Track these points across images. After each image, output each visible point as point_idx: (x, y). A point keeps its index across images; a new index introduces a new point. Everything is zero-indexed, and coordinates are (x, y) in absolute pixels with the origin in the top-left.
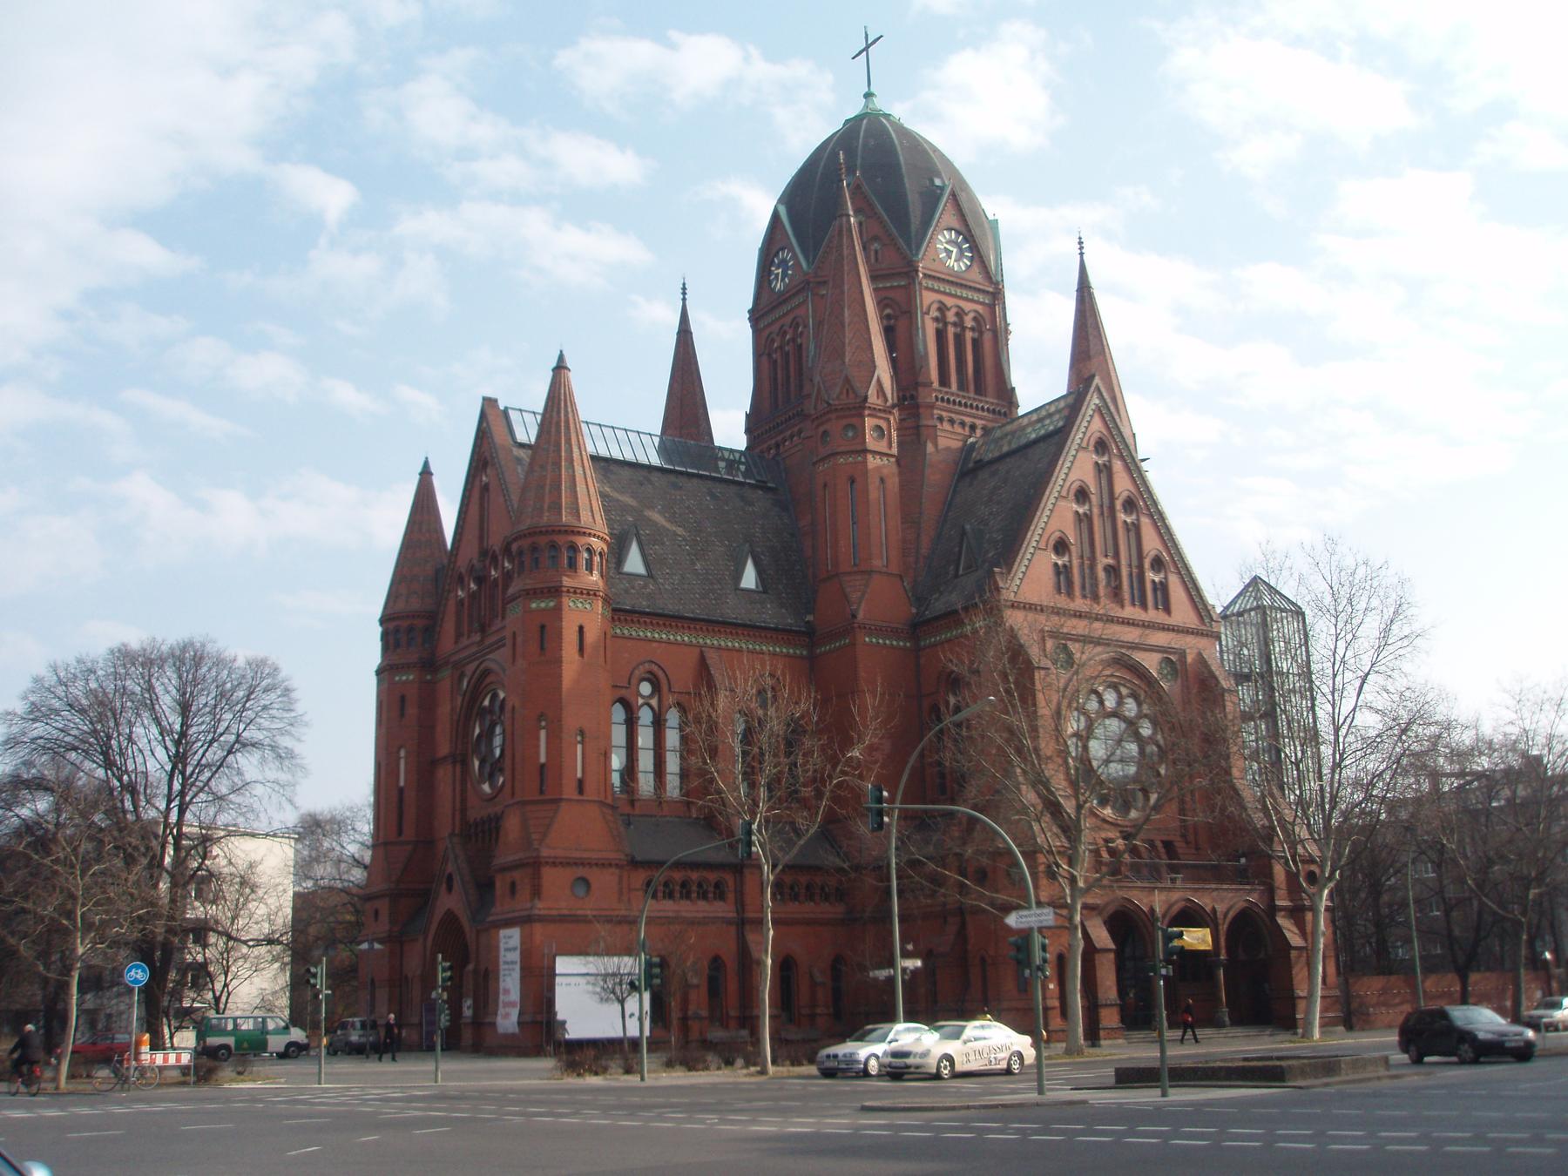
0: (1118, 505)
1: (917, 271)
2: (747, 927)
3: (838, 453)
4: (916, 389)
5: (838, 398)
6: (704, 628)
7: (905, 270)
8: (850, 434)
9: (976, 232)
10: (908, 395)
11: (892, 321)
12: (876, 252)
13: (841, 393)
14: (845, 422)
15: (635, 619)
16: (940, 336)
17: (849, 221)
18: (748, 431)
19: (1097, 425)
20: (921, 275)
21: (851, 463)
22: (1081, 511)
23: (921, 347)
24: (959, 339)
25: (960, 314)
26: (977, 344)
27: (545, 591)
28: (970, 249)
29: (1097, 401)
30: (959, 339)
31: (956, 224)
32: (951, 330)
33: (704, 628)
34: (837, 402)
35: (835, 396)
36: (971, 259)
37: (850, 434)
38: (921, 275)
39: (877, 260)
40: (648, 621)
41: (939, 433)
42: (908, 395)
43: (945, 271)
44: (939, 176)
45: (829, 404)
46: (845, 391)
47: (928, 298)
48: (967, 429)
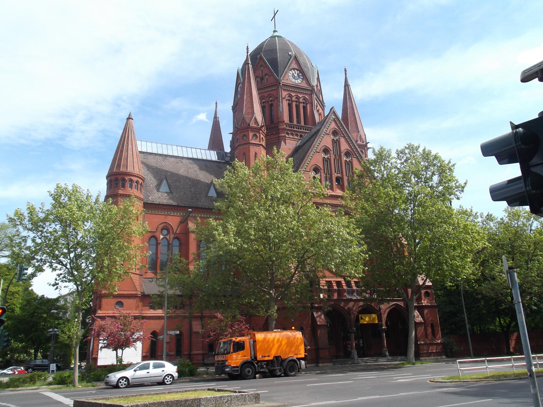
0: (342, 154)
1: (280, 83)
4: (278, 123)
5: (240, 125)
7: (276, 83)
8: (245, 138)
9: (305, 70)
10: (276, 126)
11: (272, 102)
12: (267, 79)
13: (241, 124)
14: (242, 134)
15: (160, 207)
16: (290, 105)
17: (248, 66)
18: (231, 146)
19: (333, 126)
20: (281, 85)
21: (244, 148)
22: (326, 157)
23: (281, 109)
24: (297, 107)
25: (298, 98)
26: (305, 108)
27: (113, 195)
28: (302, 75)
29: (334, 117)
30: (297, 107)
31: (296, 67)
32: (294, 104)
34: (240, 127)
36: (303, 79)
37: (245, 138)
38: (281, 85)
39: (267, 81)
40: (165, 207)
41: (287, 138)
44: (291, 51)
45: (237, 128)
47: (285, 94)
48: (299, 137)
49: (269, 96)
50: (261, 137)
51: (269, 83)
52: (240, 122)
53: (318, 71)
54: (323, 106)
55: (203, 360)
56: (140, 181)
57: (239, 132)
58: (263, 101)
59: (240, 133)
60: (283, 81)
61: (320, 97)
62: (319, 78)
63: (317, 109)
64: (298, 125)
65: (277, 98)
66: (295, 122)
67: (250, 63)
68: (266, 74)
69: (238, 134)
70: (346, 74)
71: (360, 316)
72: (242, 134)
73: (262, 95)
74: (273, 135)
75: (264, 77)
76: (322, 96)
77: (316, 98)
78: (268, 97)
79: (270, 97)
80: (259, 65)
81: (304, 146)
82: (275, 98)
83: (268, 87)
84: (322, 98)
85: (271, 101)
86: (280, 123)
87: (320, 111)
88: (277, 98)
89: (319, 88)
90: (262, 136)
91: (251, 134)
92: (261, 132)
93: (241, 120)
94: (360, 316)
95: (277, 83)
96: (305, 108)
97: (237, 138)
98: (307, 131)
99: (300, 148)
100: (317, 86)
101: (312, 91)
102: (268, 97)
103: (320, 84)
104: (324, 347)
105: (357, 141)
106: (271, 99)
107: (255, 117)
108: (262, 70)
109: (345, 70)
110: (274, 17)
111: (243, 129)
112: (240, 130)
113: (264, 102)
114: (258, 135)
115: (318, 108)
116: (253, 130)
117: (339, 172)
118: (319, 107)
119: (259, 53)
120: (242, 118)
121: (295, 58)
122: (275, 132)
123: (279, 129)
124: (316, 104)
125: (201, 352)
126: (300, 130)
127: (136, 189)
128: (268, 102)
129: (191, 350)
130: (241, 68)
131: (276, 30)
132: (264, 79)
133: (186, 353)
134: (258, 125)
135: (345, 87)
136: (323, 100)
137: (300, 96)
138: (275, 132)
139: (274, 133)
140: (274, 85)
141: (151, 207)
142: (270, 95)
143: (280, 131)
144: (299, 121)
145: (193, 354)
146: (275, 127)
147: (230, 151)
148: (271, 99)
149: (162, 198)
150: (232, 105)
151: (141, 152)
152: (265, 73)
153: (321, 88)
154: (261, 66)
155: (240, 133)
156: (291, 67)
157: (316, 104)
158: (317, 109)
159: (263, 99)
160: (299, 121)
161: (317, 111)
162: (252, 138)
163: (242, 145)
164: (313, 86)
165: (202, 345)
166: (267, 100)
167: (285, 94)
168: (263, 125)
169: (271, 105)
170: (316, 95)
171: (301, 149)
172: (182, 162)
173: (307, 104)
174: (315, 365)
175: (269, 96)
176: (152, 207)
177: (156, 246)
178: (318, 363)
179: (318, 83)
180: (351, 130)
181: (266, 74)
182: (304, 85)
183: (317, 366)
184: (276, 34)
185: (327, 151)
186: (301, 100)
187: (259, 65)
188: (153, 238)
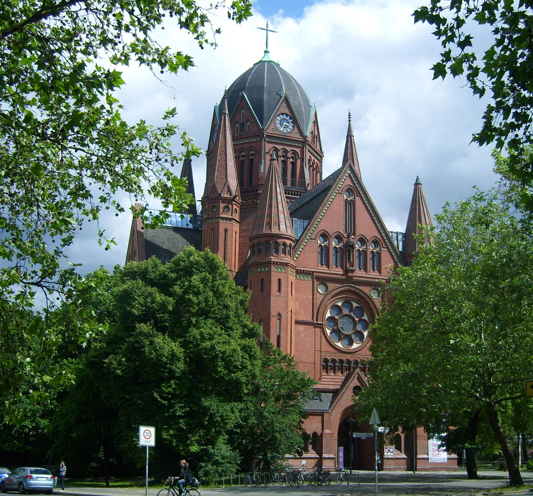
8: (215, 210)
20: (265, 136)
26: (294, 164)
31: (287, 112)
37: (215, 210)
38: (265, 136)
47: (268, 147)
50: (234, 209)
53: (316, 112)
54: (321, 157)
58: (243, 153)
60: (269, 131)
70: (350, 121)
85: (252, 155)
88: (259, 152)
90: (235, 207)
91: (222, 205)
92: (234, 203)
95: (260, 134)
96: (294, 164)
101: (304, 142)
109: (349, 115)
114: (230, 206)
121: (286, 100)
124: (308, 157)
134: (231, 195)
137: (288, 149)
148: (252, 152)
150: (207, 150)
162: (223, 211)
164: (306, 137)
167: (268, 147)
169: (252, 160)
173: (296, 160)
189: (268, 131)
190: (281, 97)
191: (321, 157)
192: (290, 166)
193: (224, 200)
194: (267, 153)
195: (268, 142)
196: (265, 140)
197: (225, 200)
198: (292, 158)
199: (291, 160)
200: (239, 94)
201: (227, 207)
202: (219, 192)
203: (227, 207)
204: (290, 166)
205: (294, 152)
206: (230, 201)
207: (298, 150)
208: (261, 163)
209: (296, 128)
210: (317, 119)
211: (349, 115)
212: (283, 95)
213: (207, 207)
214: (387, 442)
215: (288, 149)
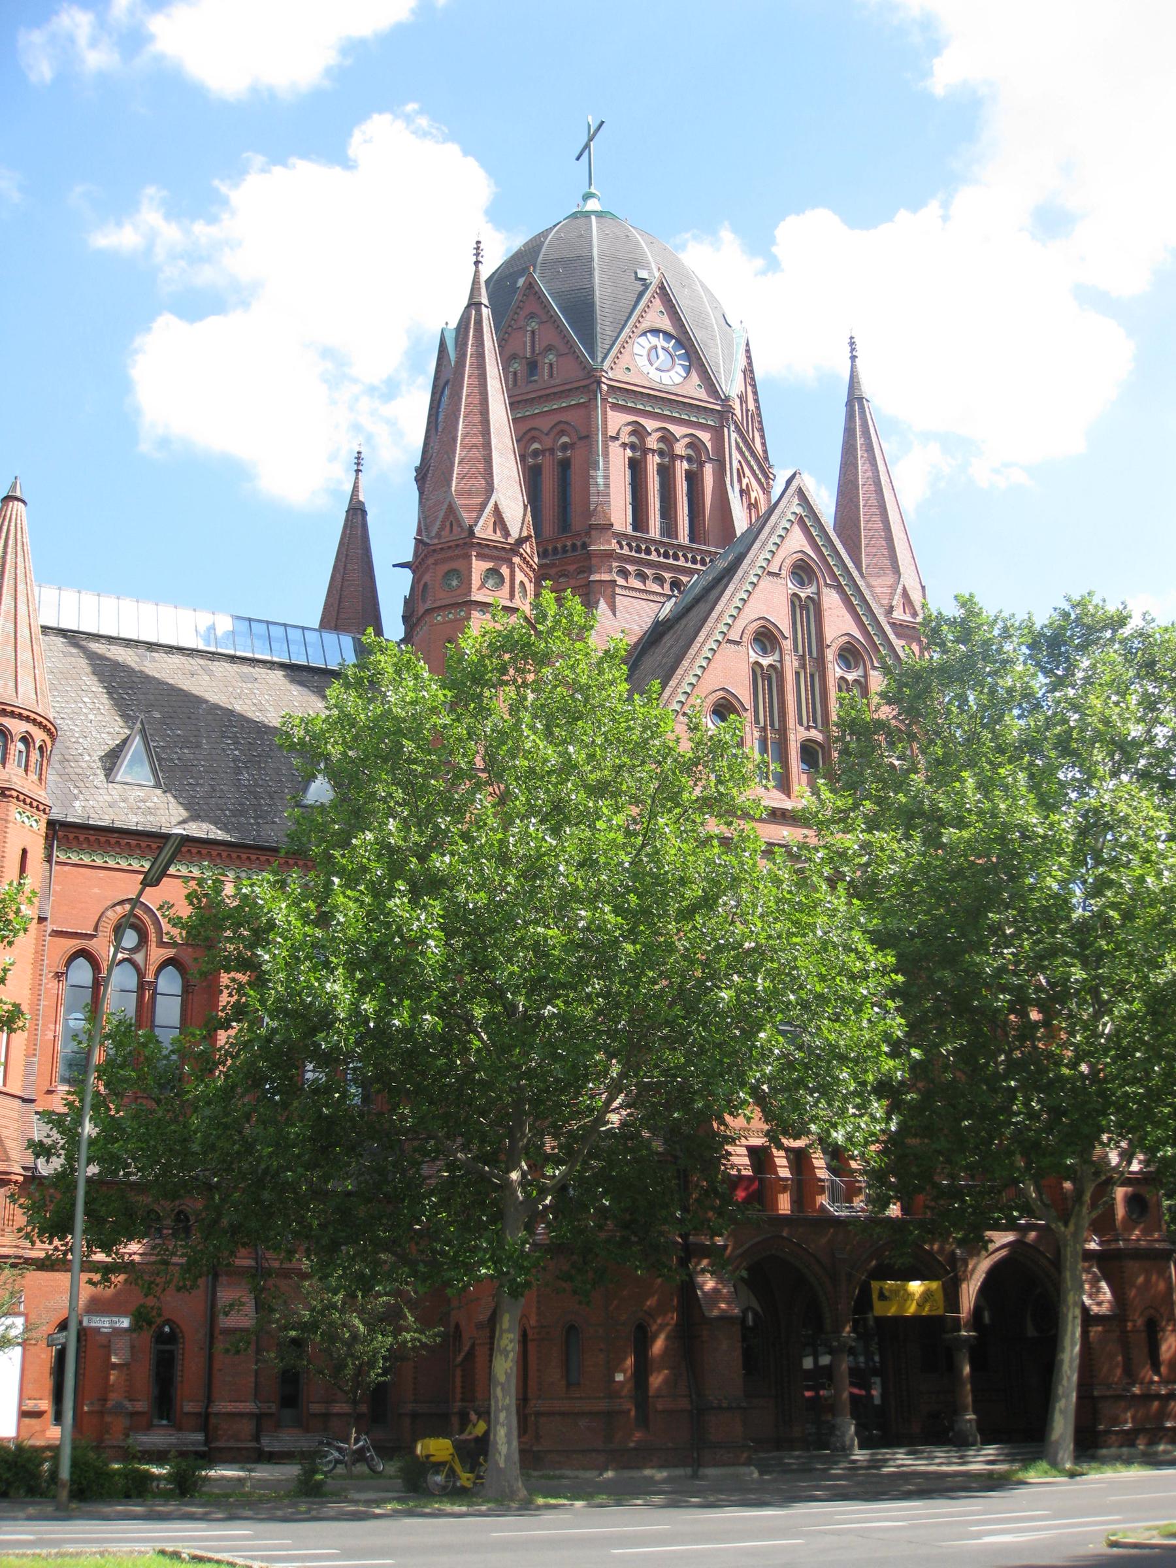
0: (830, 654)
1: (599, 382)
2: (223, 1279)
3: (433, 610)
4: (588, 534)
5: (438, 535)
6: (224, 854)
8: (455, 583)
9: (698, 335)
10: (579, 543)
11: (569, 453)
12: (551, 365)
13: (442, 528)
14: (446, 567)
15: (113, 841)
16: (636, 467)
17: (479, 314)
18: (406, 619)
19: (797, 541)
20: (605, 387)
21: (452, 621)
22: (765, 662)
23: (600, 480)
24: (666, 473)
25: (667, 438)
26: (694, 479)
28: (688, 356)
29: (799, 510)
30: (666, 473)
31: (666, 324)
32: (653, 461)
33: (224, 854)
34: (436, 541)
35: (433, 534)
36: (688, 371)
37: (455, 583)
38: (605, 387)
39: (551, 375)
40: (133, 842)
41: (618, 591)
42: (579, 543)
43: (646, 384)
44: (646, 266)
46: (448, 524)
47: (617, 421)
48: (667, 586)
49: (558, 428)
50: (517, 582)
51: (557, 381)
52: (438, 523)
53: (748, 345)
54: (767, 477)
55: (257, 1439)
56: (39, 736)
57: (430, 561)
58: (536, 446)
59: (436, 563)
60: (613, 372)
61: (753, 440)
62: (752, 371)
63: (740, 481)
64: (665, 540)
65: (587, 437)
66: (655, 530)
67: (485, 300)
68: (549, 348)
69: (428, 568)
70: (853, 358)
71: (875, 1285)
72: (446, 567)
73: (529, 424)
74: (566, 576)
75: (539, 358)
76: (763, 437)
77: (737, 444)
78: (555, 431)
79: (562, 433)
80: (523, 314)
81: (683, 622)
82: (581, 439)
83: (555, 394)
84: (764, 444)
85: (565, 447)
86: (593, 533)
87: (753, 495)
88: (586, 438)
89: (751, 406)
90: (519, 576)
91: (479, 567)
92: (516, 560)
93: (441, 514)
94: (875, 1285)
95: (590, 381)
96: (694, 479)
97: (426, 584)
98: (698, 566)
99: (670, 628)
100: (743, 399)
101: (724, 414)
102: (555, 431)
103: (755, 393)
104: (725, 1405)
105: (890, 610)
106: (565, 439)
107: (496, 506)
108: (533, 332)
109: (852, 344)
110: (587, 146)
111: (450, 547)
112: (434, 551)
113: (536, 453)
114: (505, 571)
115: (745, 481)
116: (486, 551)
117: (815, 721)
118: (748, 479)
119: (524, 271)
120: (445, 506)
121: (664, 293)
122: (575, 567)
123: (589, 555)
124: (735, 465)
125: (249, 1407)
126: (671, 561)
127: (19, 766)
128: (552, 451)
129: (209, 1400)
130: (453, 324)
131: (593, 190)
132: (540, 364)
133: (189, 1407)
134: (507, 534)
135: (850, 404)
136: (765, 451)
137: (678, 431)
138: (575, 567)
139: (571, 568)
140: (577, 388)
141: (77, 838)
142: (562, 426)
143: (594, 561)
144: (669, 528)
145: (217, 1414)
146: (574, 546)
147: (402, 636)
148: (565, 439)
149: (122, 805)
151: (45, 629)
152: (544, 344)
153: (758, 408)
154: (532, 316)
155: (436, 563)
156: (645, 325)
157: (735, 465)
158: (740, 481)
159: (534, 439)
160: (669, 528)
161: (742, 491)
162: (482, 586)
163: (439, 608)
164: (727, 398)
165: (253, 1379)
166: (548, 442)
167: (617, 421)
168: (525, 534)
169: (565, 465)
170: (738, 430)
171: (672, 632)
172: (210, 674)
173: (701, 465)
174: (689, 1471)
175: (558, 428)
176: (82, 838)
177: (93, 993)
178: (699, 1466)
179: (749, 388)
180: (868, 566)
181: (549, 348)
182: (694, 390)
183: (695, 1476)
184: (592, 205)
185: (768, 638)
186: (680, 448)
187: (523, 314)
188: (81, 960)
189: (611, 375)
190: (646, 287)
191: (767, 477)
192: (682, 487)
193: (486, 551)
194: (614, 439)
195: (615, 407)
196: (604, 400)
197: (487, 550)
198: (689, 459)
199: (685, 465)
200: (516, 282)
201: (494, 572)
202: (468, 522)
203: (494, 572)
204: (682, 487)
205: (695, 444)
206: (503, 553)
207: (705, 437)
208: (596, 465)
209: (694, 376)
210: (750, 364)
211: (852, 344)
212: (655, 283)
213: (427, 578)
214: (720, 1286)
215: (678, 431)
